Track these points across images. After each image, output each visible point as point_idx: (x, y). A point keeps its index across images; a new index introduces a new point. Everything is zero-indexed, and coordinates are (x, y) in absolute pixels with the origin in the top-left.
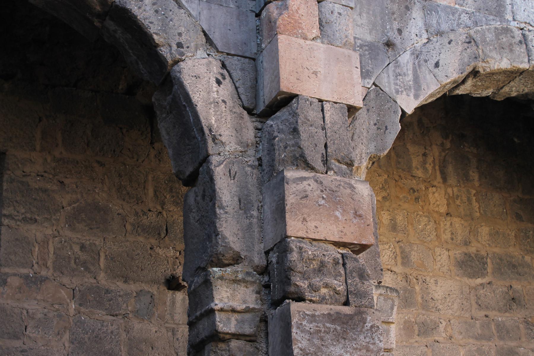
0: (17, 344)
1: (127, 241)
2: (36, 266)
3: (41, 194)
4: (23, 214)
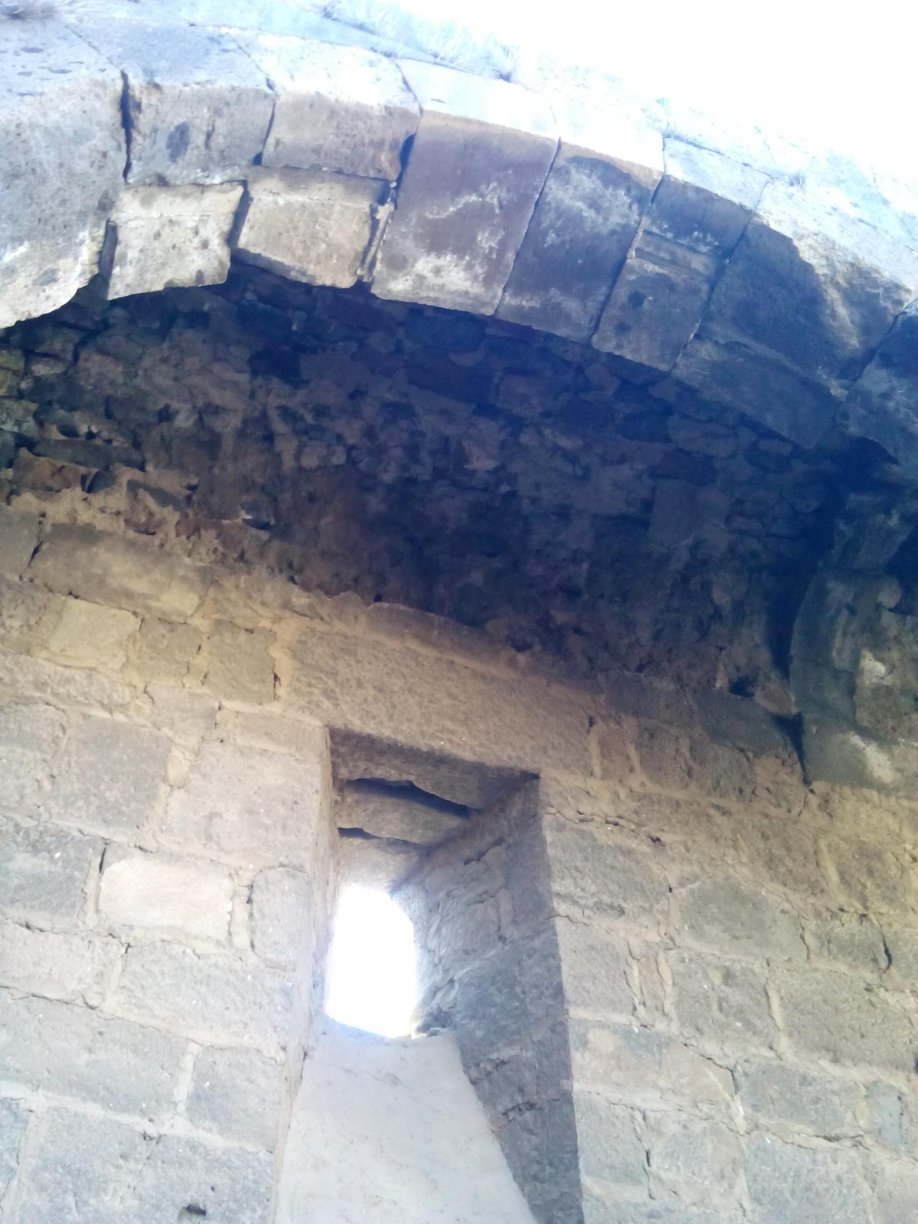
0: (635, 1194)
1: (816, 970)
2: (641, 1009)
3: (621, 858)
4: (593, 895)
